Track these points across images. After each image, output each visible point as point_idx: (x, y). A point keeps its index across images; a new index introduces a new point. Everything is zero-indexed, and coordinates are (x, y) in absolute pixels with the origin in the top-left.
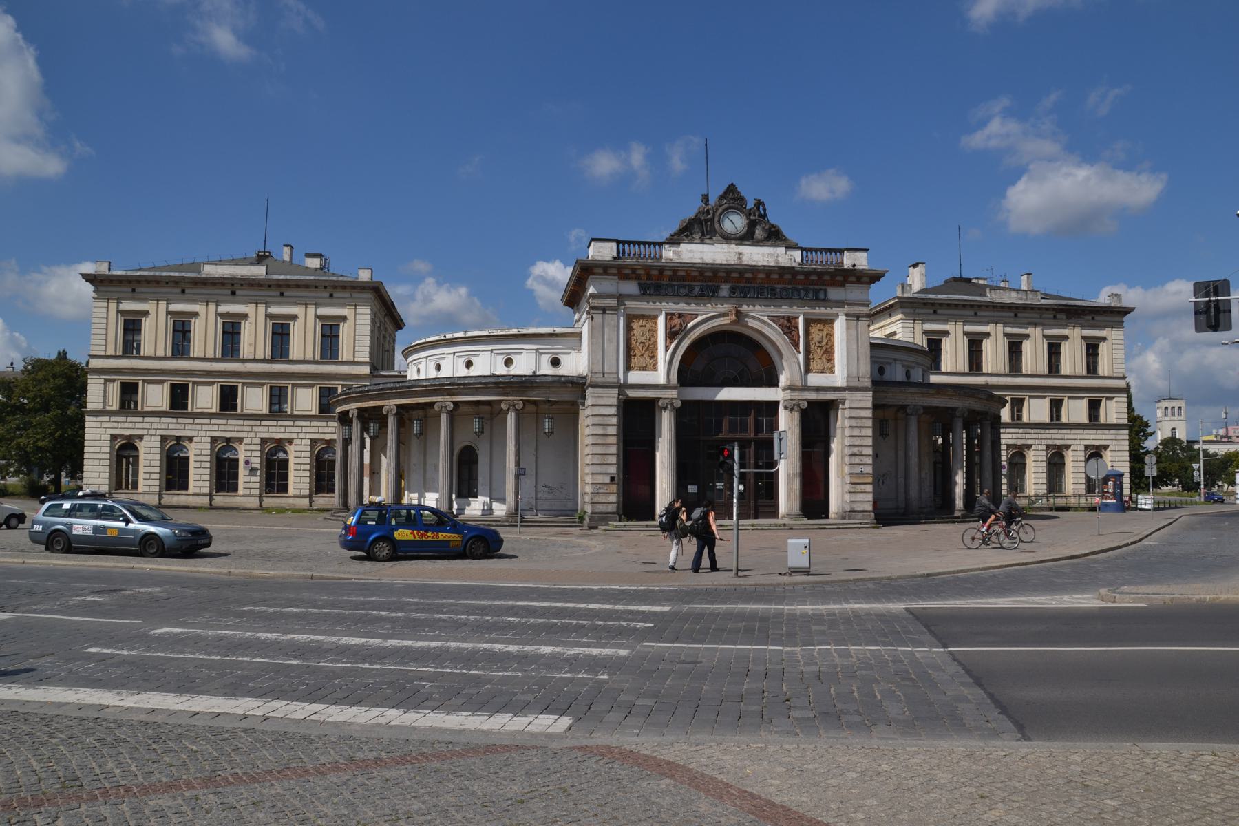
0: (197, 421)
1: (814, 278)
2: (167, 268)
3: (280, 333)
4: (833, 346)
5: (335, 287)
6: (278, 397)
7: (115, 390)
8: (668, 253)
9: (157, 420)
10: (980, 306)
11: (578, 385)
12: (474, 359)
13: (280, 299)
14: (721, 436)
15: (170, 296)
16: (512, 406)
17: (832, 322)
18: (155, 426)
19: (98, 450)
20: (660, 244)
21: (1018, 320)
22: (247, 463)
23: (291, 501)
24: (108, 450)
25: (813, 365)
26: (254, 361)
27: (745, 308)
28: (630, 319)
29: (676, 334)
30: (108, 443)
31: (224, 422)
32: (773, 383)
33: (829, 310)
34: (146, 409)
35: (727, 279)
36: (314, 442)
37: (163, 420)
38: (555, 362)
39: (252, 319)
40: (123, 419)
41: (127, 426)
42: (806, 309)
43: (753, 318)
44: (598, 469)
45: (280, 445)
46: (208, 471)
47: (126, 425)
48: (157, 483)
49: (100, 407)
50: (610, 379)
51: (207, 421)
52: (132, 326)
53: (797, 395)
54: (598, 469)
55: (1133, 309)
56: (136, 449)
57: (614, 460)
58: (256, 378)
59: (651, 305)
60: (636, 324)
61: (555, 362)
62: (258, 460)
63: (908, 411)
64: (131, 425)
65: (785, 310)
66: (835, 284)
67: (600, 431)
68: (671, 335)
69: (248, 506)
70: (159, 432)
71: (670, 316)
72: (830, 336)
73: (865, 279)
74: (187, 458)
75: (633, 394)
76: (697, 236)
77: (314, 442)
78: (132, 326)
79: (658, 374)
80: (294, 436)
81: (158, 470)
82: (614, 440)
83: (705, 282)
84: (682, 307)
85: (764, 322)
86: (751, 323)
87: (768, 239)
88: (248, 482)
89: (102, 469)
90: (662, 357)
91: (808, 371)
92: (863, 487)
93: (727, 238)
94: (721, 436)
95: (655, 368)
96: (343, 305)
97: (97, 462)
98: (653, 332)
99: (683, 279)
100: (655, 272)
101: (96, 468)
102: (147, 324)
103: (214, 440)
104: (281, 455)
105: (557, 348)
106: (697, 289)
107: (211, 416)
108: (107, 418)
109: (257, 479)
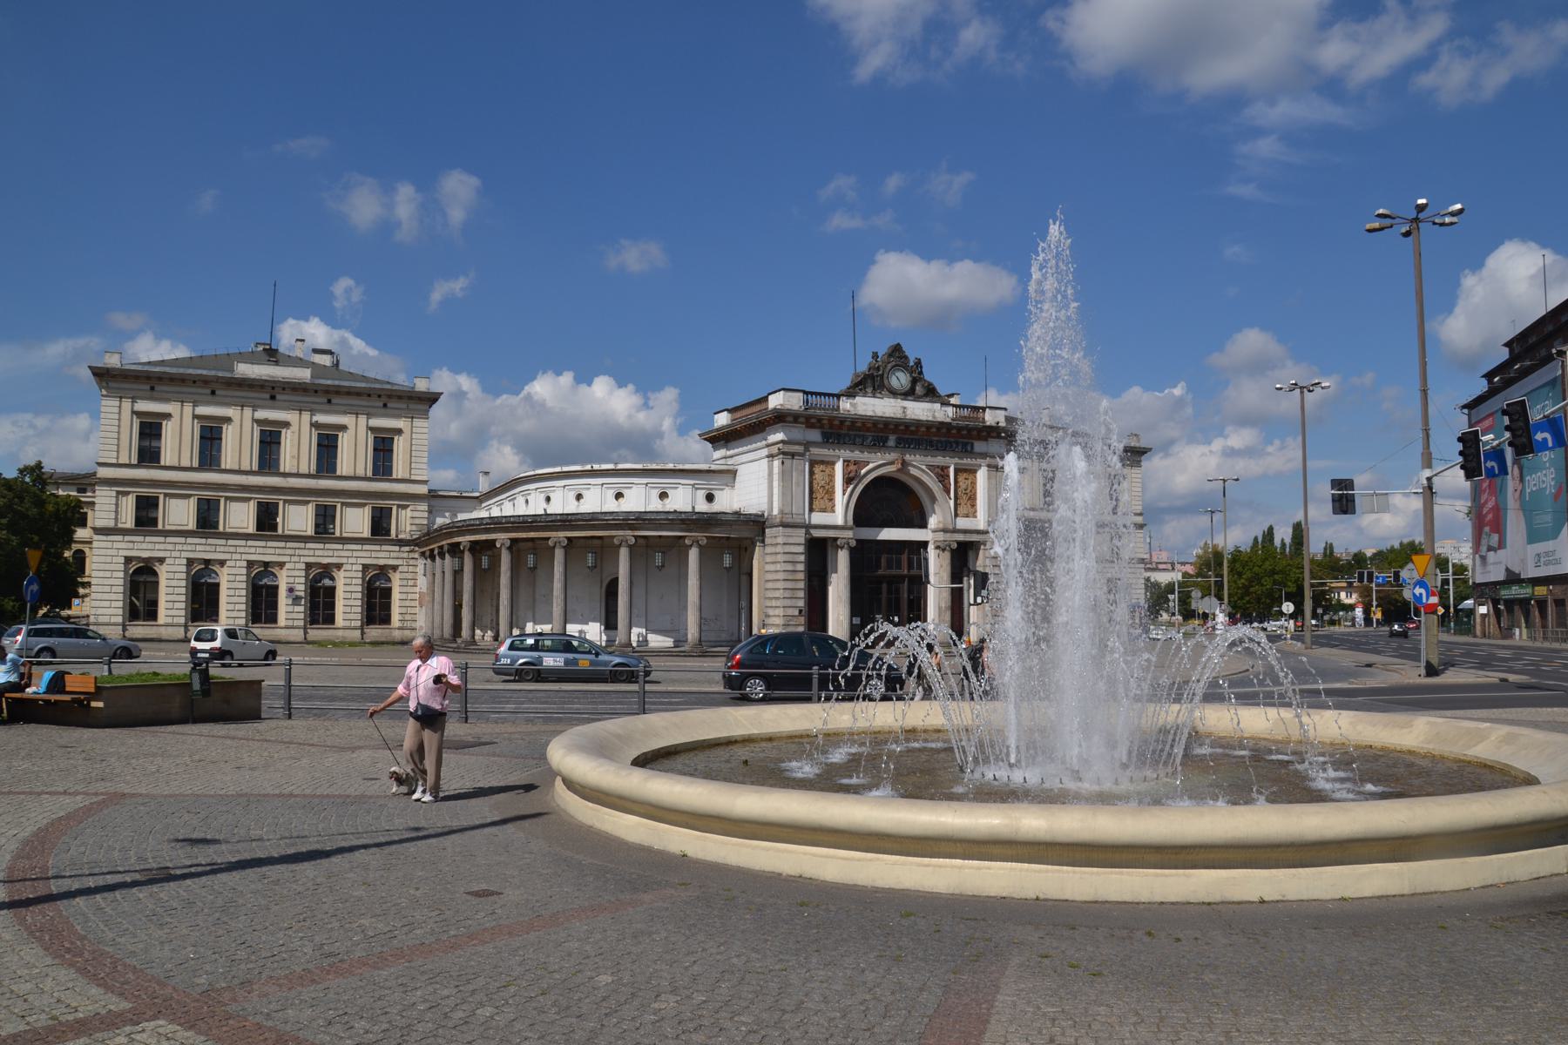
0: (231, 542)
2: (162, 363)
3: (327, 446)
5: (390, 397)
6: (325, 518)
7: (129, 505)
8: (846, 405)
9: (182, 540)
11: (756, 525)
13: (327, 407)
14: (880, 572)
15: (196, 397)
16: (696, 542)
17: (975, 472)
18: (179, 547)
19: (108, 574)
20: (838, 396)
22: (291, 590)
23: (340, 633)
24: (121, 575)
25: (961, 510)
26: (298, 475)
27: (907, 457)
28: (813, 464)
30: (122, 567)
31: (262, 543)
32: (923, 525)
33: (974, 461)
34: (168, 528)
36: (366, 567)
37: (190, 540)
38: (710, 498)
39: (295, 427)
40: (140, 538)
41: (145, 547)
42: (956, 460)
44: (788, 603)
45: (327, 571)
46: (244, 600)
47: (144, 546)
48: (183, 613)
49: (111, 524)
50: (798, 520)
51: (242, 543)
52: (150, 430)
53: (949, 537)
54: (788, 603)
56: (155, 574)
57: (801, 594)
58: (299, 495)
59: (831, 452)
60: (817, 469)
61: (710, 498)
62: (302, 587)
64: (150, 546)
65: (940, 460)
66: (980, 438)
67: (790, 567)
68: (848, 481)
69: (292, 639)
70: (185, 555)
71: (847, 462)
72: (974, 484)
74: (218, 585)
75: (817, 533)
76: (869, 390)
77: (366, 567)
78: (150, 430)
79: (838, 513)
80: (344, 560)
81: (183, 598)
82: (801, 576)
84: (857, 455)
86: (913, 471)
87: (926, 395)
88: (289, 613)
89: (114, 597)
90: (840, 499)
91: (956, 515)
93: (894, 393)
94: (880, 572)
96: (398, 417)
97: (107, 589)
98: (832, 476)
99: (859, 429)
101: (106, 596)
102: (169, 429)
103: (250, 564)
104: (327, 582)
105: (713, 484)
107: (247, 537)
108: (120, 538)
109: (302, 609)
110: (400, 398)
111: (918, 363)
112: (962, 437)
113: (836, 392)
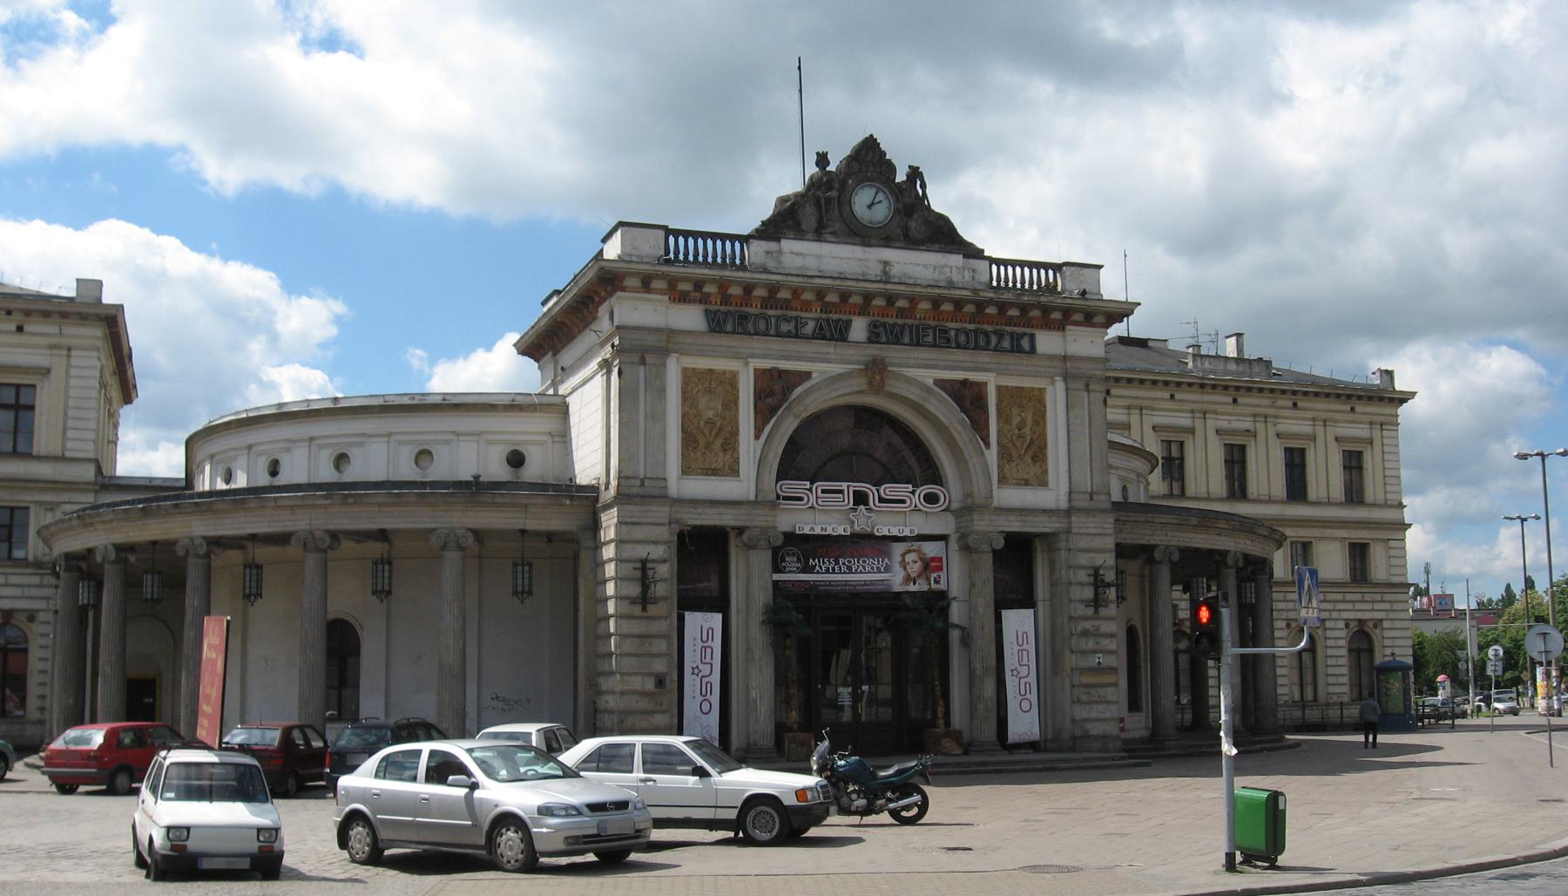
1: (1013, 312)
4: (1043, 435)
10: (1178, 384)
12: (354, 453)
20: (744, 239)
21: (1238, 409)
29: (773, 410)
35: (863, 311)
43: (908, 380)
55: (1413, 394)
63: (1157, 555)
66: (1047, 325)
73: (1099, 319)
83: (826, 313)
85: (928, 390)
90: (748, 447)
92: (1101, 691)
95: (734, 471)
99: (786, 305)
100: (735, 291)
106: (811, 324)
110: (46, 314)
111: (915, 174)
112: (1011, 321)
113: (745, 230)
